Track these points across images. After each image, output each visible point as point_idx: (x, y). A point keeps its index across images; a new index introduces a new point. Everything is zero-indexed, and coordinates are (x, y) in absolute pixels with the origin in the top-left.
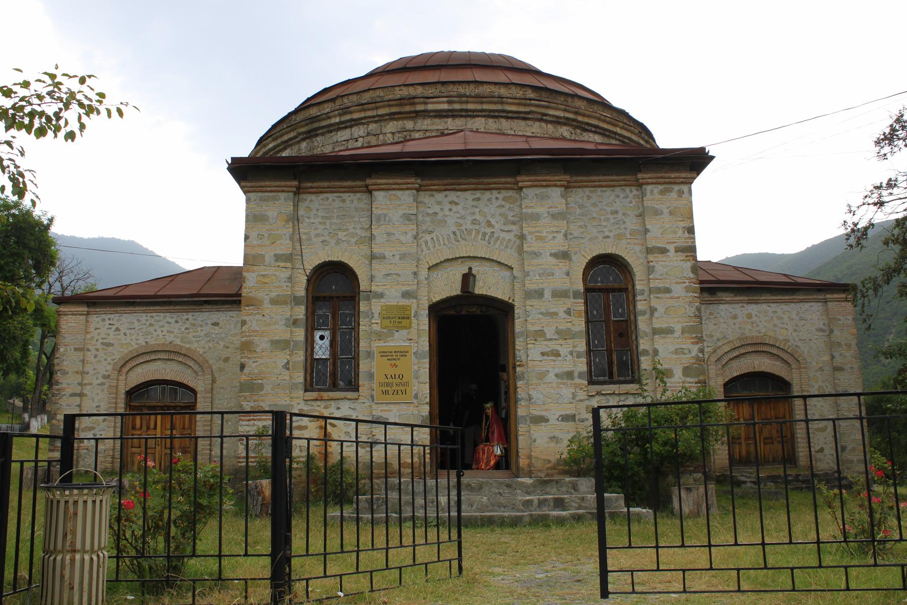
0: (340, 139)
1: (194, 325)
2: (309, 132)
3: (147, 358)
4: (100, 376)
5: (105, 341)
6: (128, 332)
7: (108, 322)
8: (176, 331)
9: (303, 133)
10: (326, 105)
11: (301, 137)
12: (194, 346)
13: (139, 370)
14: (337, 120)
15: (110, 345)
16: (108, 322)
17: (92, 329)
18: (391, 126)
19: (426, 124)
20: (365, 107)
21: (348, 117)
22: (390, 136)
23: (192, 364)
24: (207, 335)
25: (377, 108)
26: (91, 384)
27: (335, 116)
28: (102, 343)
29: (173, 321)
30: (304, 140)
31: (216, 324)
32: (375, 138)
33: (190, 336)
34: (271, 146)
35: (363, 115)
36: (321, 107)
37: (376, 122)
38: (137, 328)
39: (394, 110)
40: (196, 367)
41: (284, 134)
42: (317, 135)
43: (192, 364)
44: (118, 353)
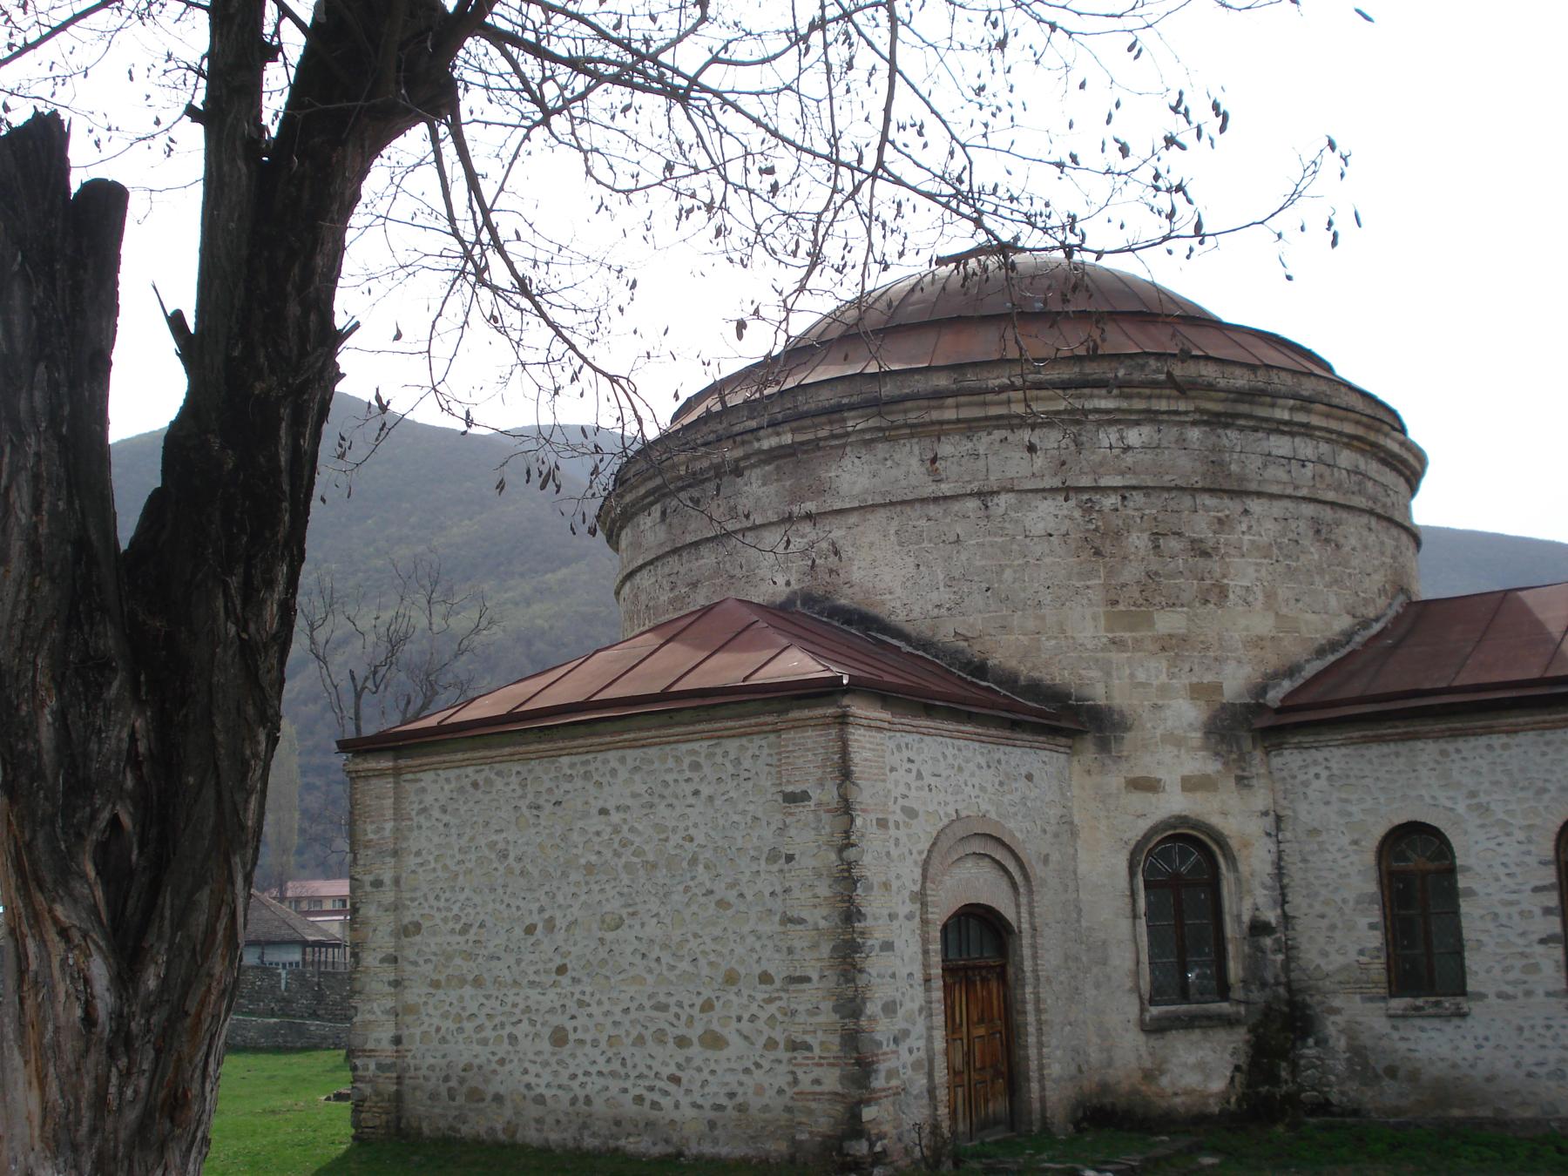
0: (1275, 452)
2: (1218, 415)
5: (906, 803)
6: (933, 781)
8: (989, 786)
10: (1238, 371)
11: (1197, 417)
12: (1011, 825)
13: (948, 881)
14: (1286, 416)
16: (906, 754)
18: (1346, 458)
20: (1335, 411)
21: (1301, 417)
25: (1342, 420)
27: (1283, 407)
28: (903, 809)
30: (1194, 423)
31: (1029, 777)
35: (1323, 423)
36: (1228, 370)
37: (1328, 441)
38: (944, 774)
39: (1360, 432)
41: (1159, 397)
42: (1226, 426)
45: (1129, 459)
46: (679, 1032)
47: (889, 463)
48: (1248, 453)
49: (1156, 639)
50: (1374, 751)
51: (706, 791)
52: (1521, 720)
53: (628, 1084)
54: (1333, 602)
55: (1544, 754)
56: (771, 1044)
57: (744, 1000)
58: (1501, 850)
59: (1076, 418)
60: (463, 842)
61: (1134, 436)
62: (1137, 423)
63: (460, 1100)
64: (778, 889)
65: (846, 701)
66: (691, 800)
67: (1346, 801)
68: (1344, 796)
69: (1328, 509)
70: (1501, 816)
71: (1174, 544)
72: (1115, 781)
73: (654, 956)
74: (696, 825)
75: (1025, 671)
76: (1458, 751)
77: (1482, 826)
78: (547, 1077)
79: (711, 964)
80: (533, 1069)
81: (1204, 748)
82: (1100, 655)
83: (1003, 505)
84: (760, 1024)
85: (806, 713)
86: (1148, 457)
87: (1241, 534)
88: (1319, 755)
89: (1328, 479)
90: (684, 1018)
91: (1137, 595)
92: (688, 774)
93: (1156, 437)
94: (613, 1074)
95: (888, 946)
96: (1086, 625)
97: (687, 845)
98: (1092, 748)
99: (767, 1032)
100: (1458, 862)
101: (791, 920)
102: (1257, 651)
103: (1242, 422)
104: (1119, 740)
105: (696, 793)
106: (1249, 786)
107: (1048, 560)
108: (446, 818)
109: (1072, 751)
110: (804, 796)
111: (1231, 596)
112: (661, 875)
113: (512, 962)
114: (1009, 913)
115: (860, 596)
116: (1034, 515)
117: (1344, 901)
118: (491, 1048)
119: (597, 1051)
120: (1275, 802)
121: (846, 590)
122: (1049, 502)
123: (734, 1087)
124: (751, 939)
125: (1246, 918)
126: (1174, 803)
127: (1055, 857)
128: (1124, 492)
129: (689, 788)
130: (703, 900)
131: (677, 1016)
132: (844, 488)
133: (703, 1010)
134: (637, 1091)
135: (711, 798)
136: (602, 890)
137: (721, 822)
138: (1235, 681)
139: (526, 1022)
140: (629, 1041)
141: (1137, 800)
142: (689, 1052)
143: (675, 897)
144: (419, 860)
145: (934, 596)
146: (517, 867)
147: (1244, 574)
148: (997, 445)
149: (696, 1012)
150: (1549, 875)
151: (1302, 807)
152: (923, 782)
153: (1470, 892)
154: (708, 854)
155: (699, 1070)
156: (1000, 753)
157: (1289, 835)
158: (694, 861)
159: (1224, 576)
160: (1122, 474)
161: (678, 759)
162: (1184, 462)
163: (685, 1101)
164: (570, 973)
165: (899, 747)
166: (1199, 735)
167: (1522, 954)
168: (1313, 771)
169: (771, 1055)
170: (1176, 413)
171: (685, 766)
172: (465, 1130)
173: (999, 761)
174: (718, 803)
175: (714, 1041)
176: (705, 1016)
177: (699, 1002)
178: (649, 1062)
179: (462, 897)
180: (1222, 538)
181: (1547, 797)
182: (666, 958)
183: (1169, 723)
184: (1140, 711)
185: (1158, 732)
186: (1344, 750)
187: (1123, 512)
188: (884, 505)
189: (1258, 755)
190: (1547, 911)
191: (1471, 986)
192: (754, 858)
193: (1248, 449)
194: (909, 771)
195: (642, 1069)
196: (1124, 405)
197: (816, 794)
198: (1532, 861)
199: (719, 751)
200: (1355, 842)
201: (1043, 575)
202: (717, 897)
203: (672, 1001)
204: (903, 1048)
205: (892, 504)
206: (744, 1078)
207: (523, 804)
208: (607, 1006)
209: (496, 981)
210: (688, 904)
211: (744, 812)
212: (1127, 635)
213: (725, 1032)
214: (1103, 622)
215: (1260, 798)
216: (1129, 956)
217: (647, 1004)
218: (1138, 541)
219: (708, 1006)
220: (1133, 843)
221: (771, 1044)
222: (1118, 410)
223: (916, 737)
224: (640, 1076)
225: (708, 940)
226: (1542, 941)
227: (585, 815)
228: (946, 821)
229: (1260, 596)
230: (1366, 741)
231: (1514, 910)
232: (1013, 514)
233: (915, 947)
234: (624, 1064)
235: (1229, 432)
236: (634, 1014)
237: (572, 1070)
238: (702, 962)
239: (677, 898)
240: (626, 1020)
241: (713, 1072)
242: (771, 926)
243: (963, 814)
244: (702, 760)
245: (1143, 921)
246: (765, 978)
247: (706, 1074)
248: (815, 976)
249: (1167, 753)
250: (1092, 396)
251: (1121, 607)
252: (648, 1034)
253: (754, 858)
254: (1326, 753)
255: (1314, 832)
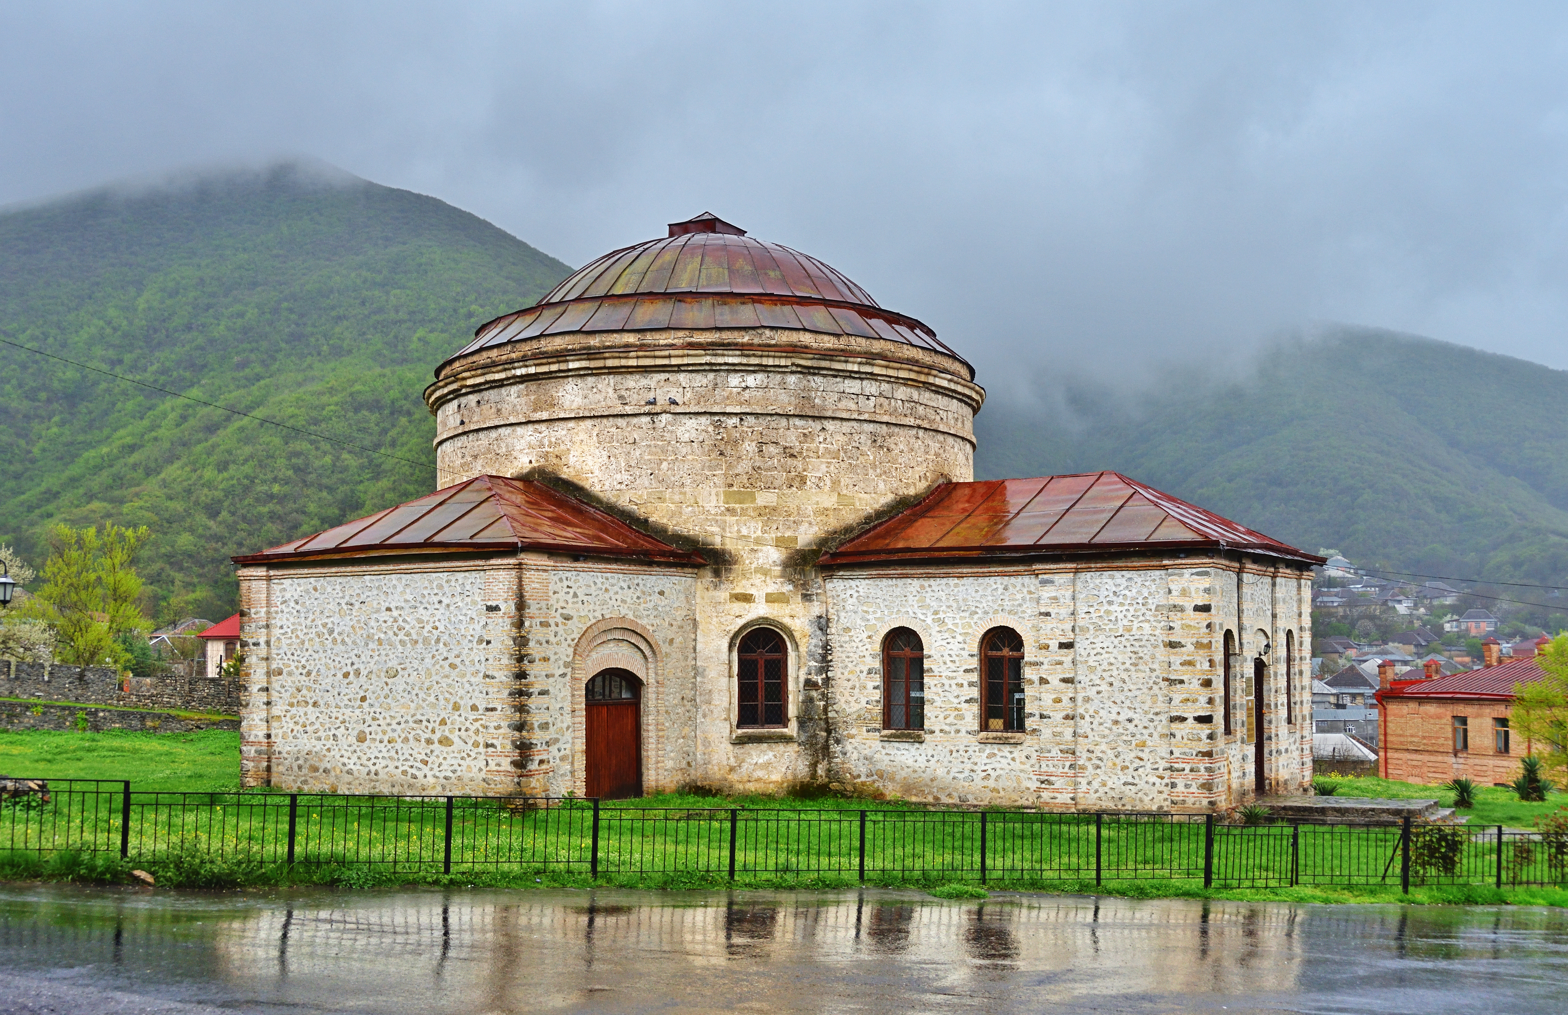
1: (644, 593)
3: (604, 638)
4: (561, 663)
5: (564, 611)
6: (585, 598)
7: (566, 583)
8: (629, 600)
9: (798, 366)
11: (794, 368)
12: (644, 622)
13: (594, 655)
15: (567, 618)
16: (566, 583)
17: (551, 594)
19: (927, 397)
22: (900, 402)
23: (643, 646)
24: (655, 608)
26: (553, 676)
28: (562, 615)
29: (625, 586)
31: (661, 593)
32: (887, 401)
33: (641, 608)
34: (731, 360)
38: (594, 594)
40: (647, 652)
41: (768, 356)
43: (643, 646)
44: (576, 628)
45: (746, 394)
46: (427, 736)
47: (595, 390)
48: (826, 392)
49: (755, 509)
50: (885, 582)
51: (446, 601)
52: (965, 571)
53: (399, 764)
54: (881, 486)
55: (977, 591)
56: (476, 744)
57: (463, 719)
58: (949, 646)
59: (712, 368)
60: (308, 622)
61: (751, 380)
62: (754, 372)
63: (305, 771)
64: (483, 659)
65: (522, 556)
66: (437, 606)
67: (866, 612)
68: (865, 608)
69: (884, 426)
70: (950, 626)
71: (772, 449)
72: (723, 594)
73: (414, 693)
74: (439, 620)
75: (674, 525)
76: (930, 586)
77: (940, 632)
78: (354, 759)
79: (446, 699)
80: (346, 754)
81: (782, 577)
82: (719, 518)
83: (664, 421)
84: (471, 733)
85: (499, 561)
86: (761, 393)
87: (818, 443)
88: (853, 583)
89: (886, 407)
90: (430, 728)
91: (746, 481)
92: (436, 591)
93: (766, 381)
94: (391, 758)
95: (542, 693)
96: (712, 499)
97: (434, 631)
98: (710, 574)
99: (474, 737)
100: (925, 652)
101: (488, 676)
102: (823, 518)
103: (825, 372)
104: (729, 571)
105: (440, 602)
106: (810, 601)
107: (690, 457)
108: (298, 607)
109: (697, 576)
110: (496, 608)
111: (808, 483)
112: (420, 645)
113: (336, 694)
114: (641, 674)
115: (573, 473)
116: (683, 429)
117: (861, 672)
118: (323, 742)
119: (383, 745)
120: (827, 611)
121: (565, 469)
122: (693, 420)
123: (456, 767)
124: (467, 685)
125: (802, 680)
126: (759, 610)
127: (678, 640)
128: (741, 416)
129: (436, 599)
130: (442, 663)
131: (427, 727)
132: (567, 405)
133: (440, 724)
134: (404, 768)
135: (448, 606)
136: (387, 655)
137: (453, 619)
138: (807, 535)
139: (343, 728)
140: (399, 740)
141: (737, 607)
142: (432, 747)
143: (426, 660)
144: (282, 631)
145: (618, 477)
146: (339, 639)
147: (817, 469)
148: (662, 383)
149: (436, 725)
150: (974, 663)
151: (842, 614)
152: (586, 597)
153: (930, 670)
154: (445, 638)
155: (438, 757)
156: (638, 579)
157: (833, 630)
158: (438, 641)
159: (804, 470)
160: (741, 404)
161: (431, 582)
162: (784, 397)
163: (429, 774)
164: (368, 701)
165: (561, 580)
166: (779, 568)
167: (956, 709)
168: (849, 592)
169: (476, 750)
170: (779, 366)
171: (435, 583)
172: (306, 789)
173: (638, 585)
174: (452, 608)
175: (445, 741)
176: (442, 727)
177: (438, 720)
178: (411, 752)
179: (307, 654)
180: (805, 446)
181: (976, 617)
182: (422, 695)
183: (761, 561)
184: (742, 553)
185: (753, 566)
186: (867, 581)
187: (740, 428)
188: (590, 417)
189: (820, 580)
190: (971, 684)
191: (927, 726)
192: (470, 641)
193: (829, 389)
194: (568, 593)
195: (407, 756)
196: (744, 361)
197: (503, 607)
198: (965, 654)
199: (453, 579)
200: (870, 637)
201: (686, 467)
202: (449, 661)
203: (424, 718)
204: (553, 749)
205: (594, 417)
206: (462, 762)
207: (343, 602)
208: (388, 720)
209: (327, 705)
210: (434, 665)
211: (466, 615)
212: (737, 506)
213: (451, 736)
214: (722, 498)
215: (816, 609)
216: (726, 699)
217: (411, 720)
218: (749, 447)
219: (443, 722)
220: (731, 634)
221: (476, 744)
222: (740, 364)
223: (575, 573)
224: (406, 760)
225: (444, 685)
226: (966, 701)
227: (378, 611)
228: (594, 621)
229: (828, 482)
230: (880, 577)
231: (953, 682)
232: (669, 427)
233: (567, 692)
234: (397, 753)
235: (816, 378)
236: (403, 725)
237: (368, 755)
238: (441, 697)
239: (428, 661)
240: (398, 728)
241: (445, 758)
242: (479, 678)
243: (607, 616)
244: (444, 584)
245: (735, 679)
246: (474, 708)
247: (441, 760)
248: (499, 709)
249: (758, 579)
250: (723, 355)
251: (735, 488)
252: (411, 737)
253: (470, 641)
254: (857, 582)
255: (847, 630)
